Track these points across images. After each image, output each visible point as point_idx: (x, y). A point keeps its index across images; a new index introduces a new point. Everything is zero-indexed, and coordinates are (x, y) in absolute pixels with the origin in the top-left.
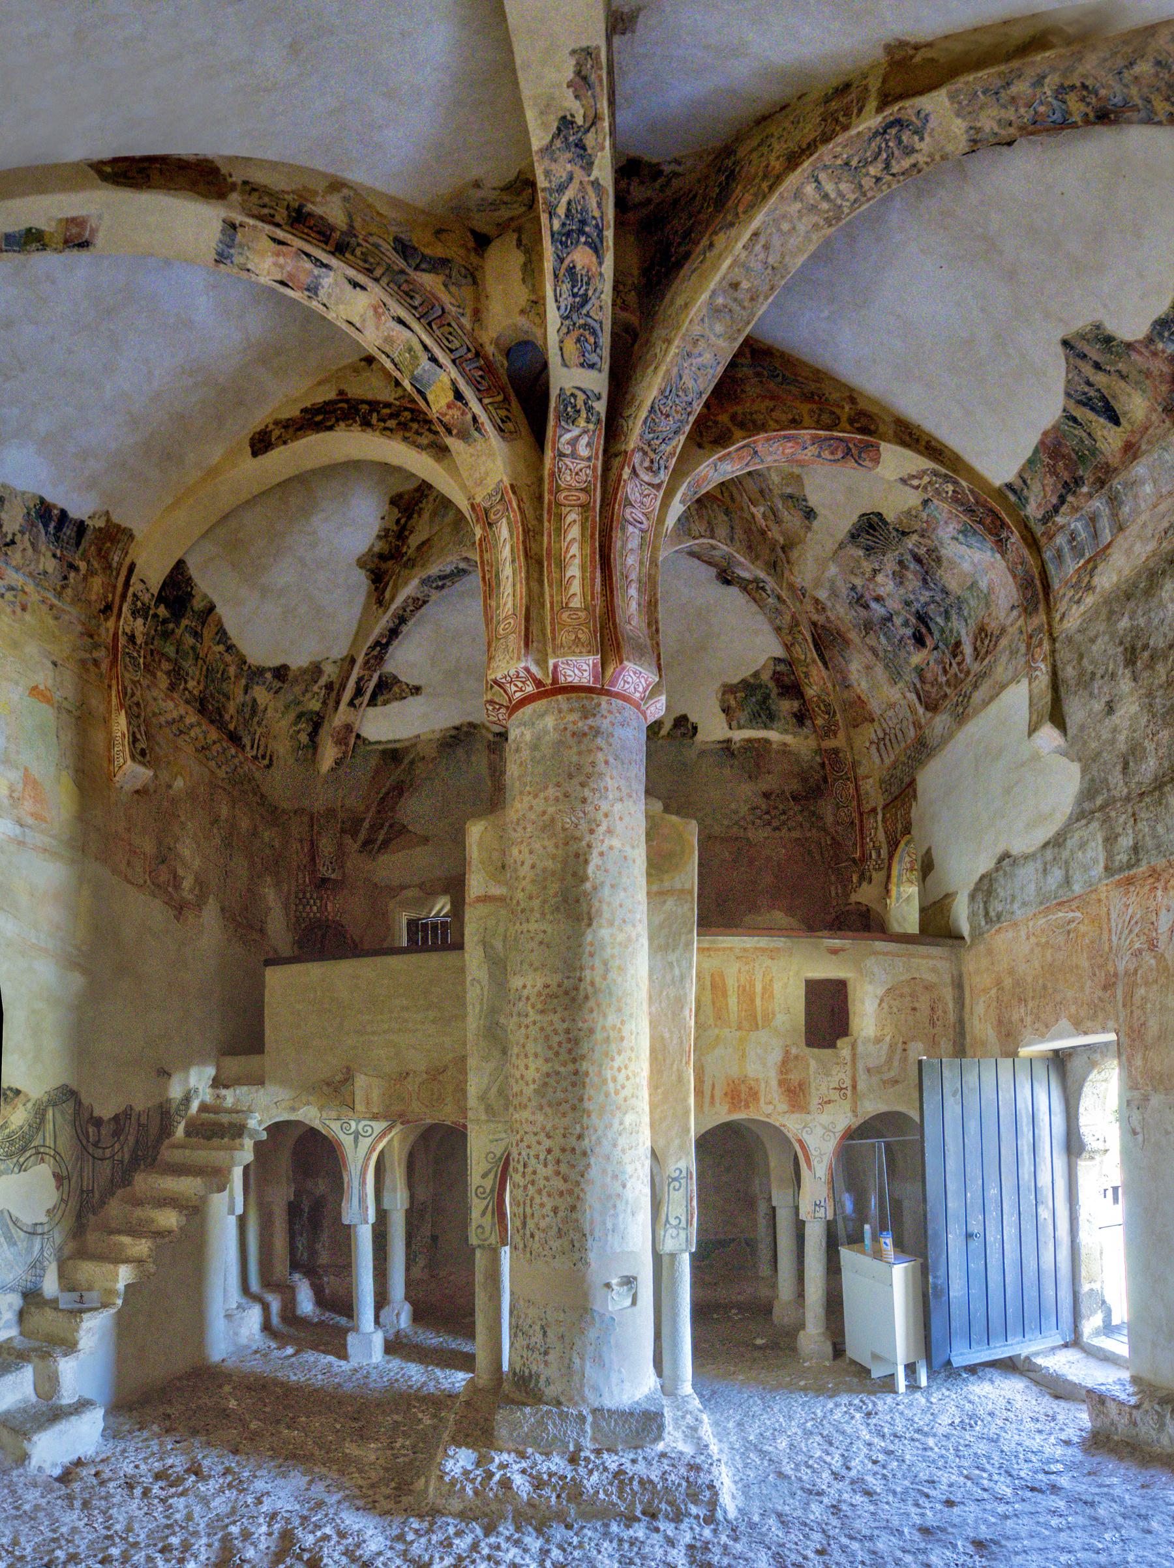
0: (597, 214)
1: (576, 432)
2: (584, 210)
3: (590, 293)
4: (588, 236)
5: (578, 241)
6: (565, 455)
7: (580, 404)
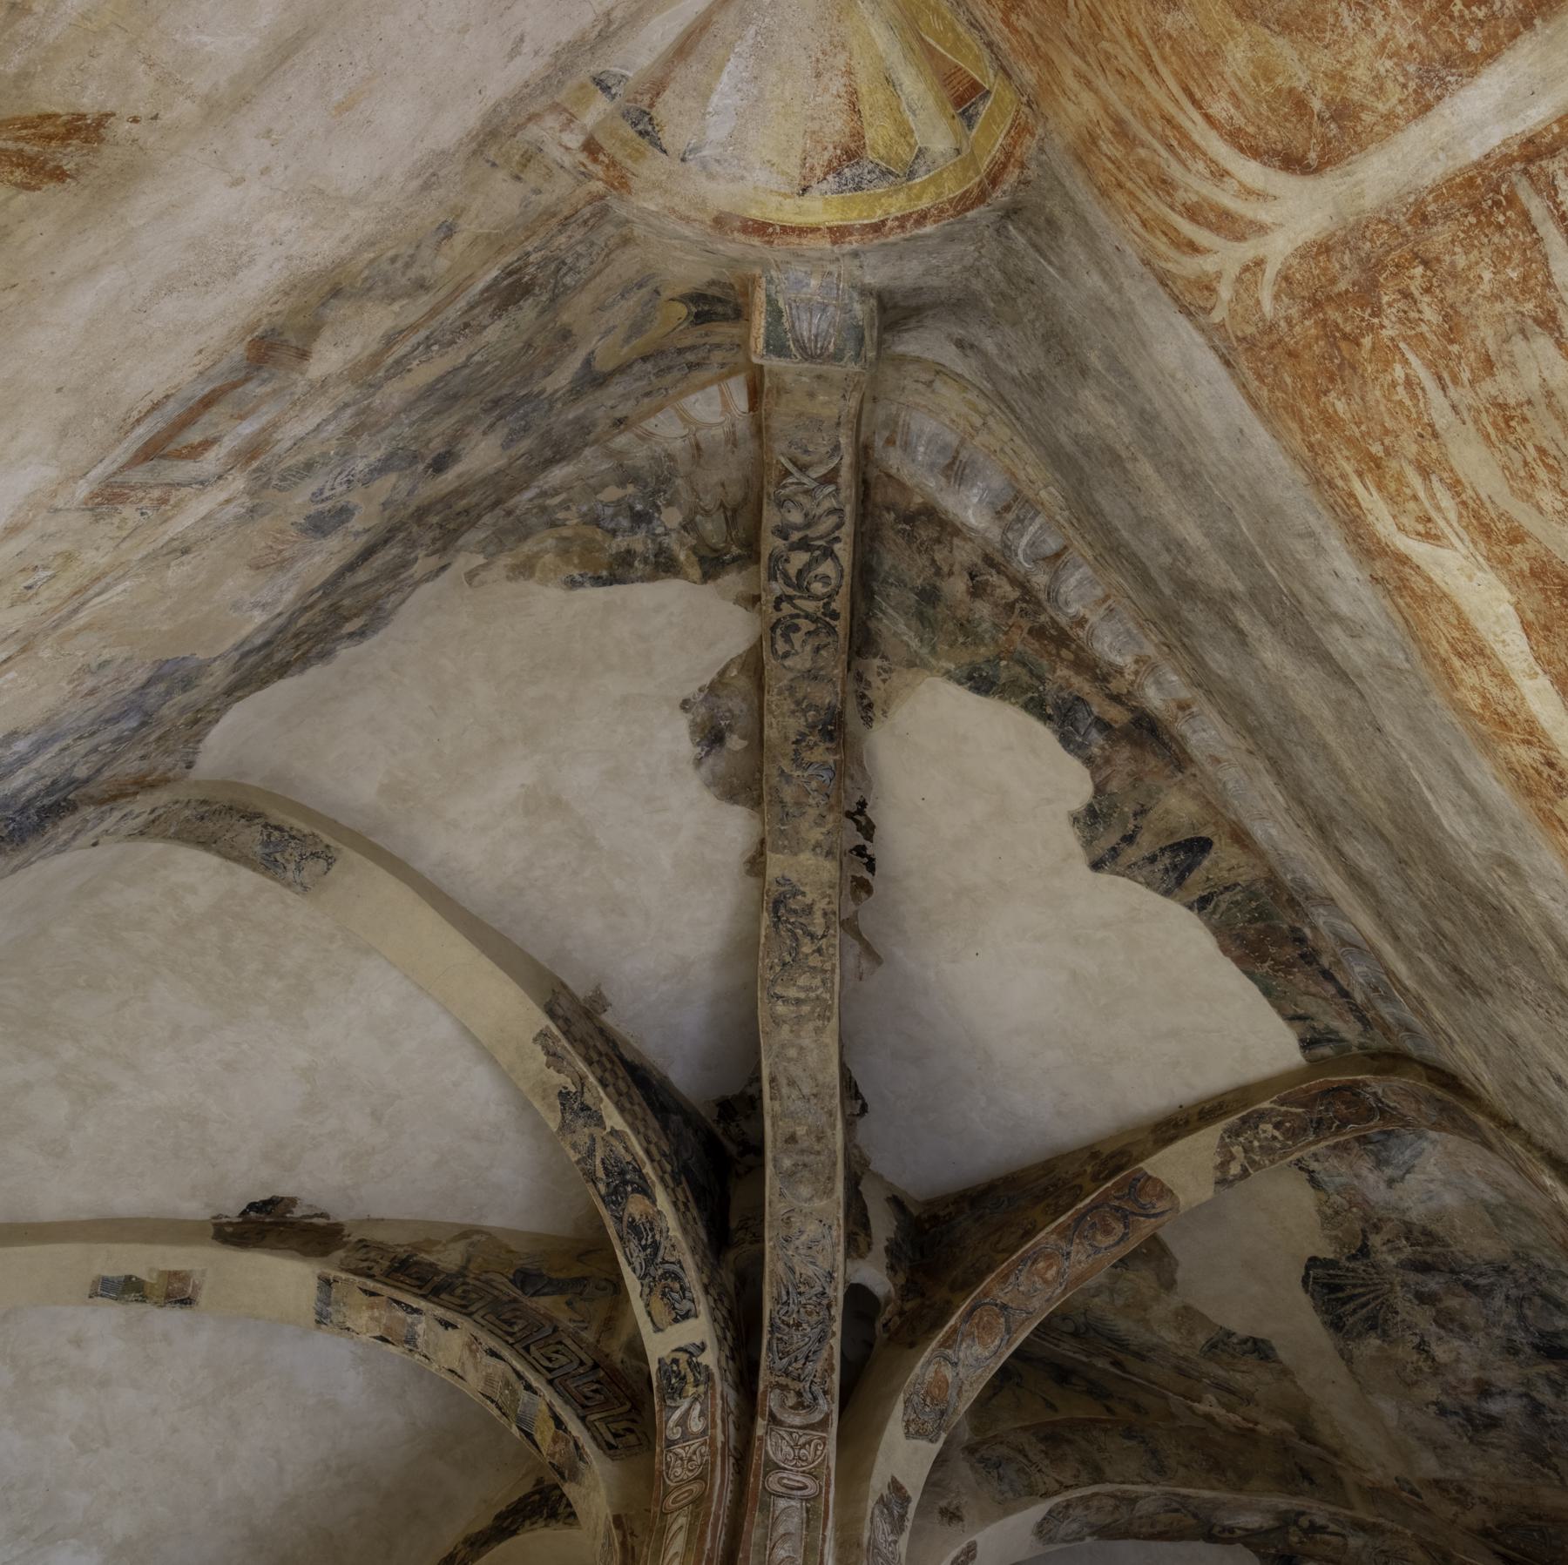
0: (629, 1158)
1: (685, 1404)
2: (618, 1161)
4: (632, 1183)
5: (626, 1192)
6: (674, 1443)
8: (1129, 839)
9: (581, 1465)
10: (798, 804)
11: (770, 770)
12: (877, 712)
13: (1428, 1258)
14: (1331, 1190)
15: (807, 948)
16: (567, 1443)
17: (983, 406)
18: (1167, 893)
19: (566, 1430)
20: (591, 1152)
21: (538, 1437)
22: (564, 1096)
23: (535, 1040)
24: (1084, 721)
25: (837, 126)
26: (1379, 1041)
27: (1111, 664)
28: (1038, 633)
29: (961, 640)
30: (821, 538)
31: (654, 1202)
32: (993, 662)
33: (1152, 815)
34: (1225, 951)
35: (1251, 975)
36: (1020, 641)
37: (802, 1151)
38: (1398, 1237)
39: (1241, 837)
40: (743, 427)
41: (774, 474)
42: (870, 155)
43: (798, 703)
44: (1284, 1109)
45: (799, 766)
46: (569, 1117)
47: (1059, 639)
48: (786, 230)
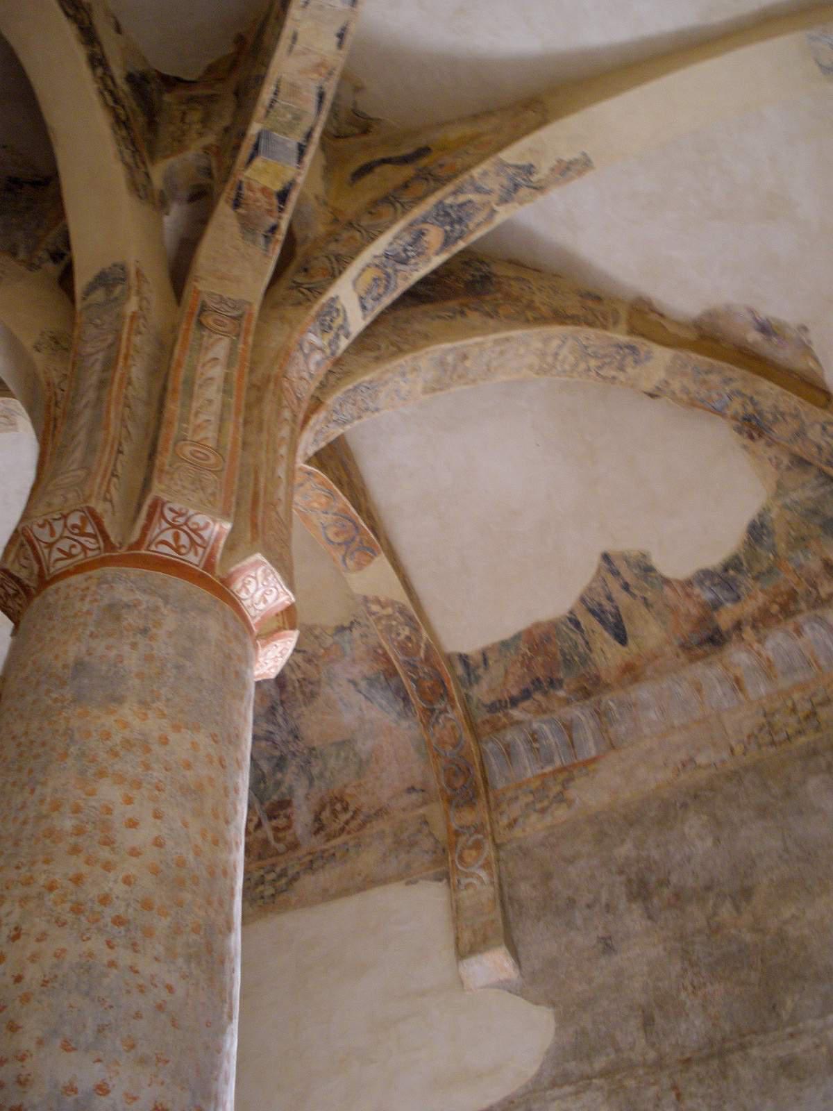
0: (471, 226)
2: (469, 216)
3: (413, 261)
7: (335, 325)
8: (626, 587)
9: (261, 240)
10: (704, 382)
11: (737, 372)
12: (747, 442)
13: (290, 688)
14: (337, 638)
15: (593, 363)
16: (270, 212)
18: (583, 600)
19: (281, 210)
20: (478, 190)
21: (258, 162)
22: (529, 170)
23: (584, 154)
24: (723, 595)
26: (482, 716)
27: (766, 637)
28: (793, 595)
29: (793, 533)
31: (437, 254)
32: (773, 548)
33: (644, 610)
34: (537, 625)
35: (517, 637)
36: (787, 580)
37: (455, 368)
38: (304, 673)
39: (631, 673)
43: (783, 414)
44: (423, 645)
45: (732, 392)
46: (511, 171)
47: (785, 607)
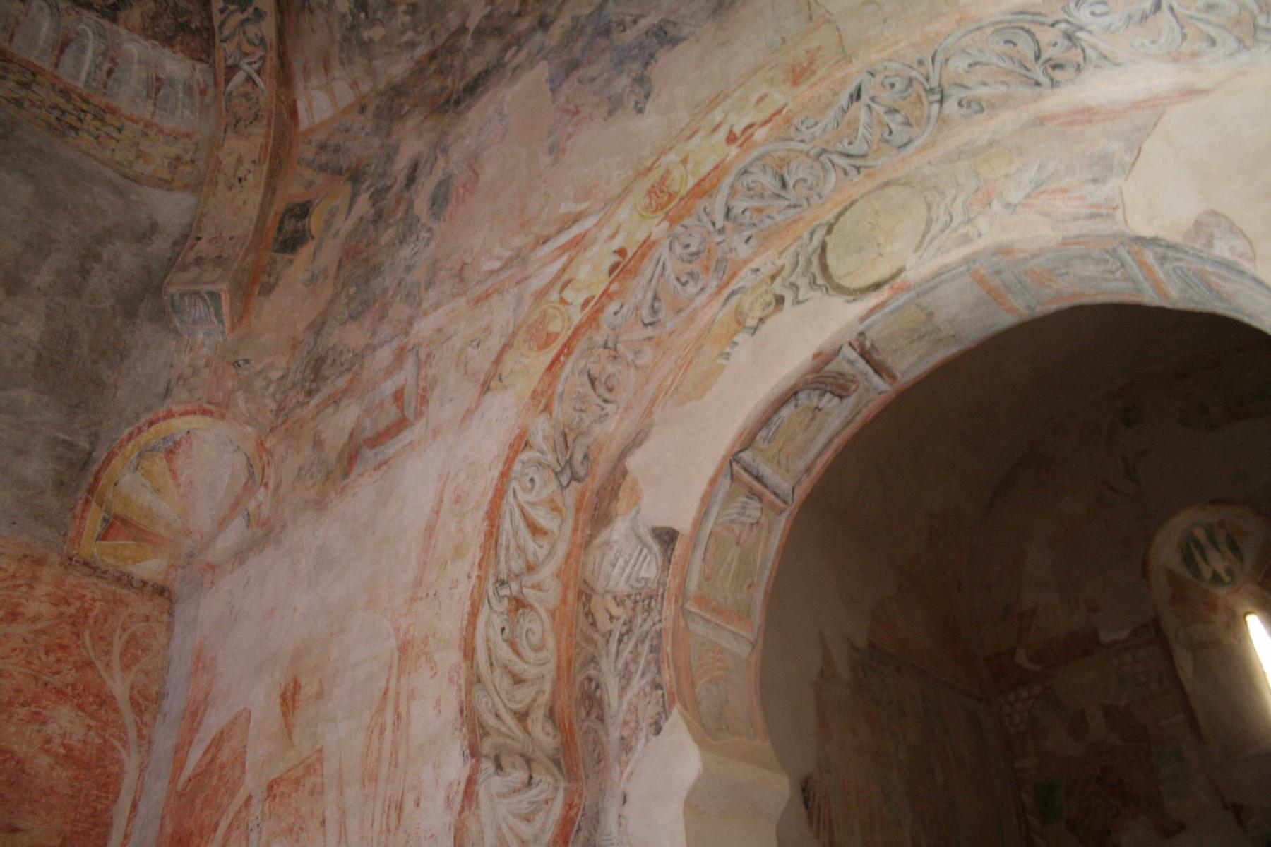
17: (140, 168)
25: (180, 461)
30: (232, 12)
40: (299, 84)
41: (268, 70)
42: (162, 455)
48: (194, 413)
